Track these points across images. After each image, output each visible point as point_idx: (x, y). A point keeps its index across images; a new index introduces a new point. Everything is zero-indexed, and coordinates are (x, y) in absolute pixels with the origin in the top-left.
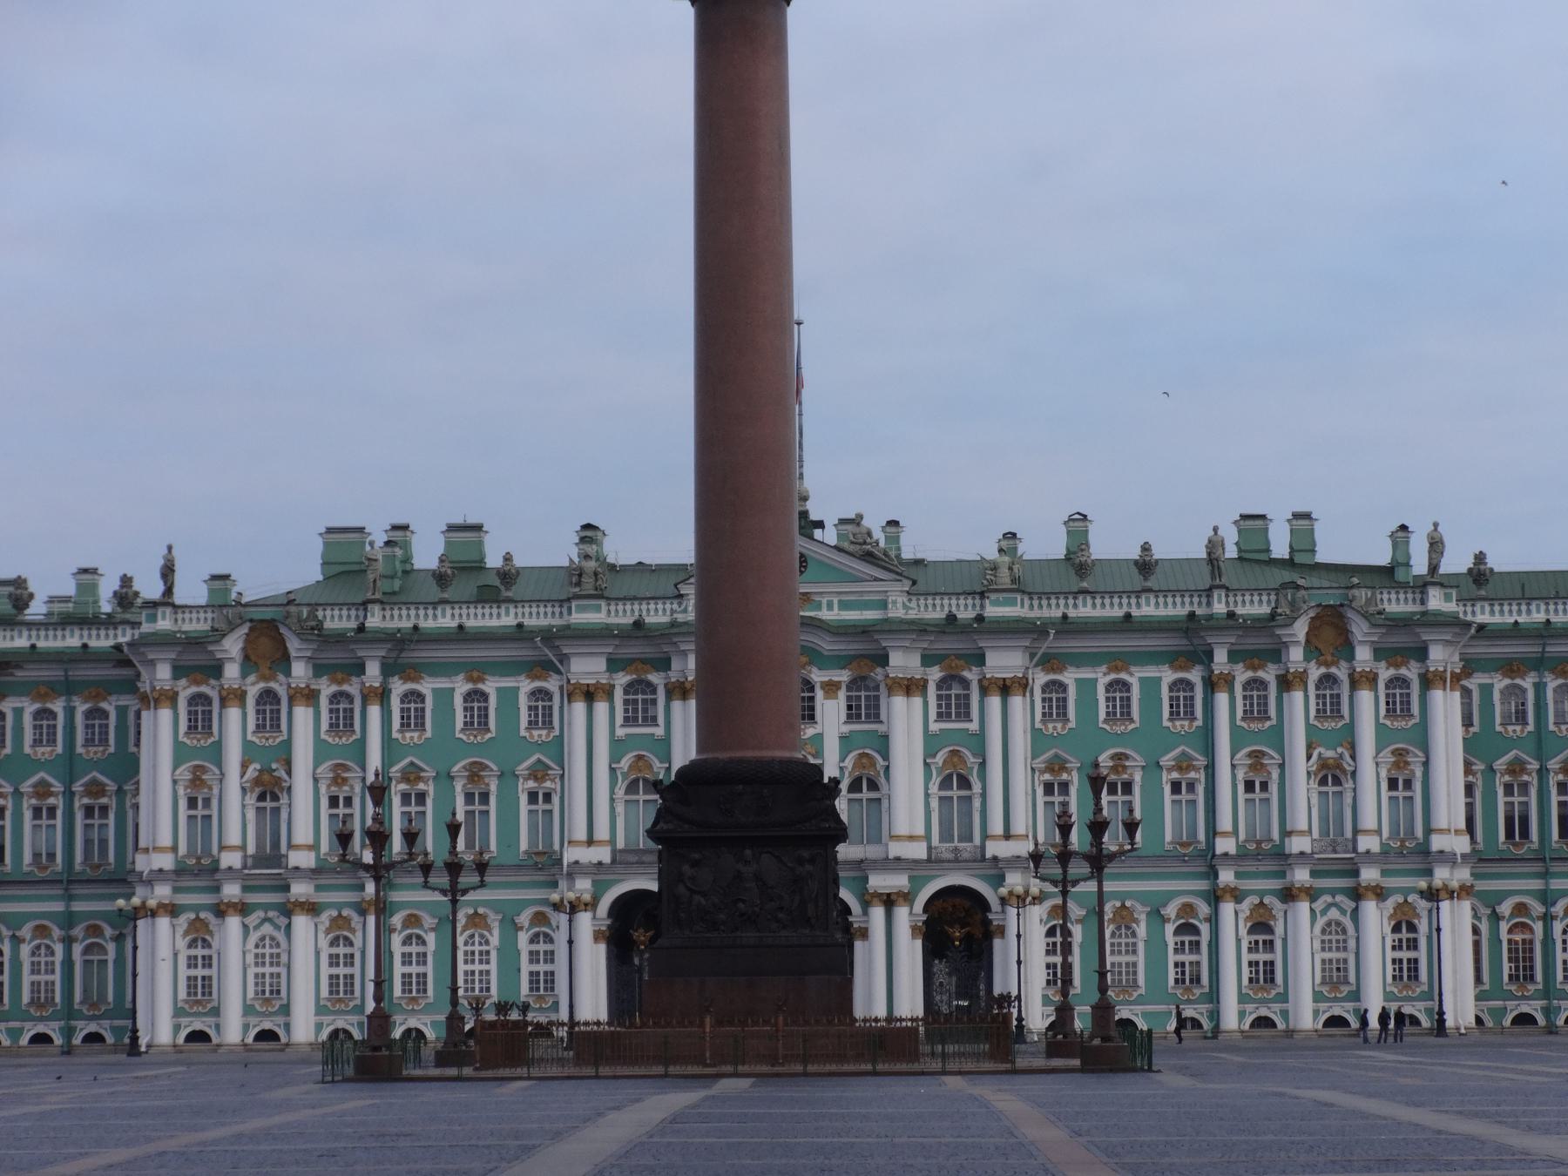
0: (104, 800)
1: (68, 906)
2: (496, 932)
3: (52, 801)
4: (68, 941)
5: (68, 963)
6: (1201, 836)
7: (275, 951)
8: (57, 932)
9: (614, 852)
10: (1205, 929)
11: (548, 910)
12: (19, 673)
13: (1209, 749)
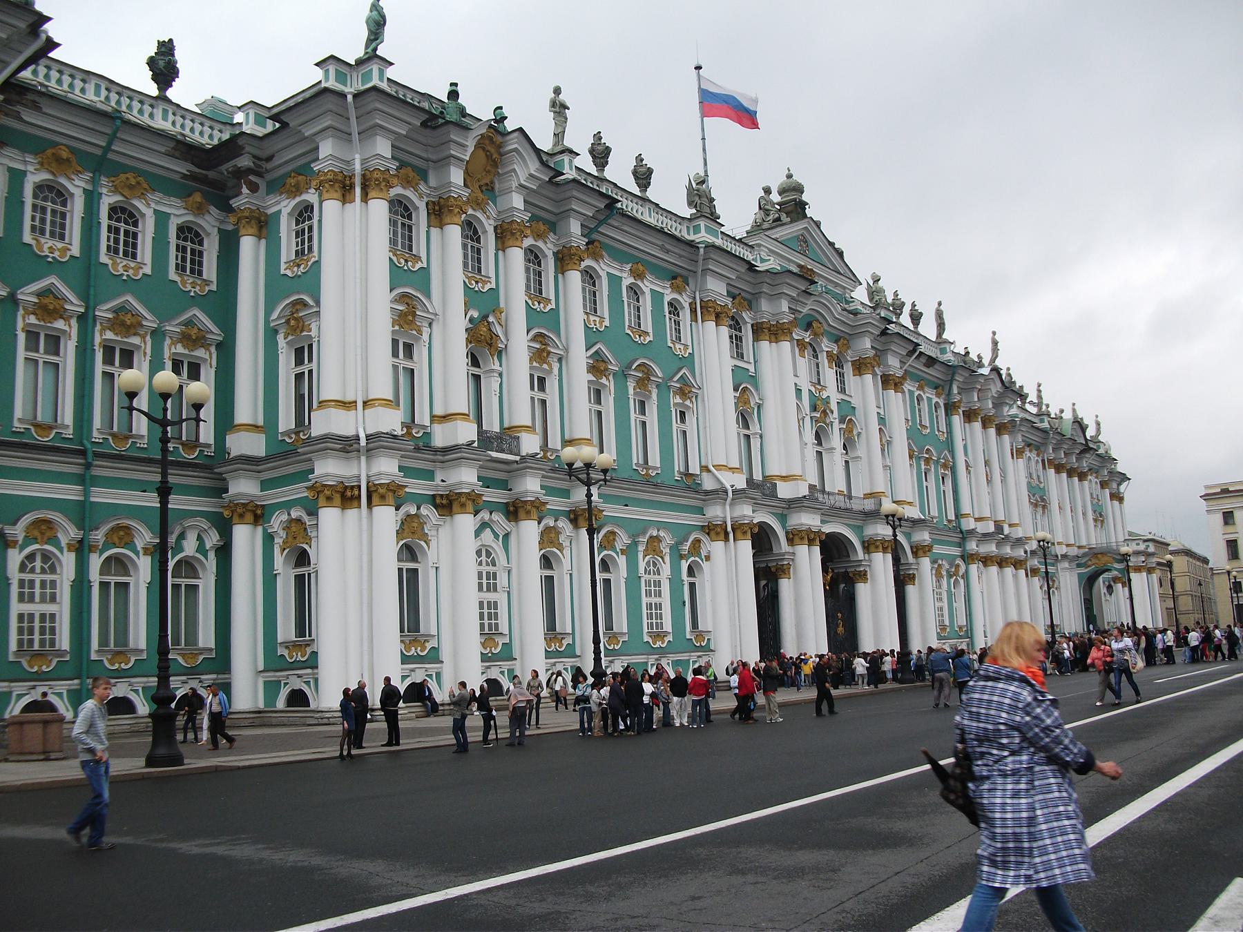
0: (135, 340)
1: (86, 493)
2: (667, 559)
3: (60, 324)
4: (81, 549)
5: (81, 586)
6: (952, 516)
7: (491, 569)
8: (68, 532)
9: (750, 481)
10: (962, 581)
11: (704, 538)
12: (29, 116)
13: (952, 452)
